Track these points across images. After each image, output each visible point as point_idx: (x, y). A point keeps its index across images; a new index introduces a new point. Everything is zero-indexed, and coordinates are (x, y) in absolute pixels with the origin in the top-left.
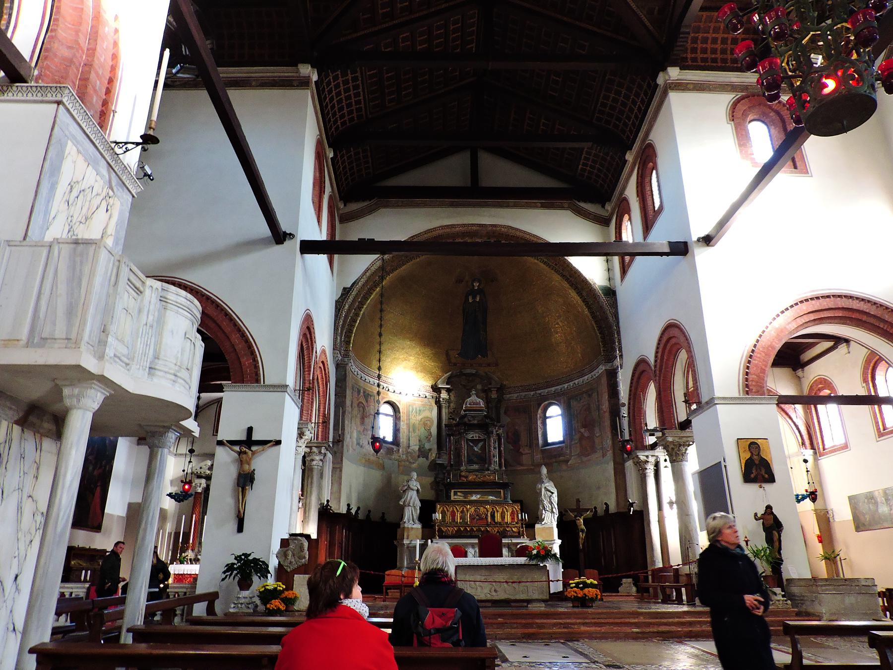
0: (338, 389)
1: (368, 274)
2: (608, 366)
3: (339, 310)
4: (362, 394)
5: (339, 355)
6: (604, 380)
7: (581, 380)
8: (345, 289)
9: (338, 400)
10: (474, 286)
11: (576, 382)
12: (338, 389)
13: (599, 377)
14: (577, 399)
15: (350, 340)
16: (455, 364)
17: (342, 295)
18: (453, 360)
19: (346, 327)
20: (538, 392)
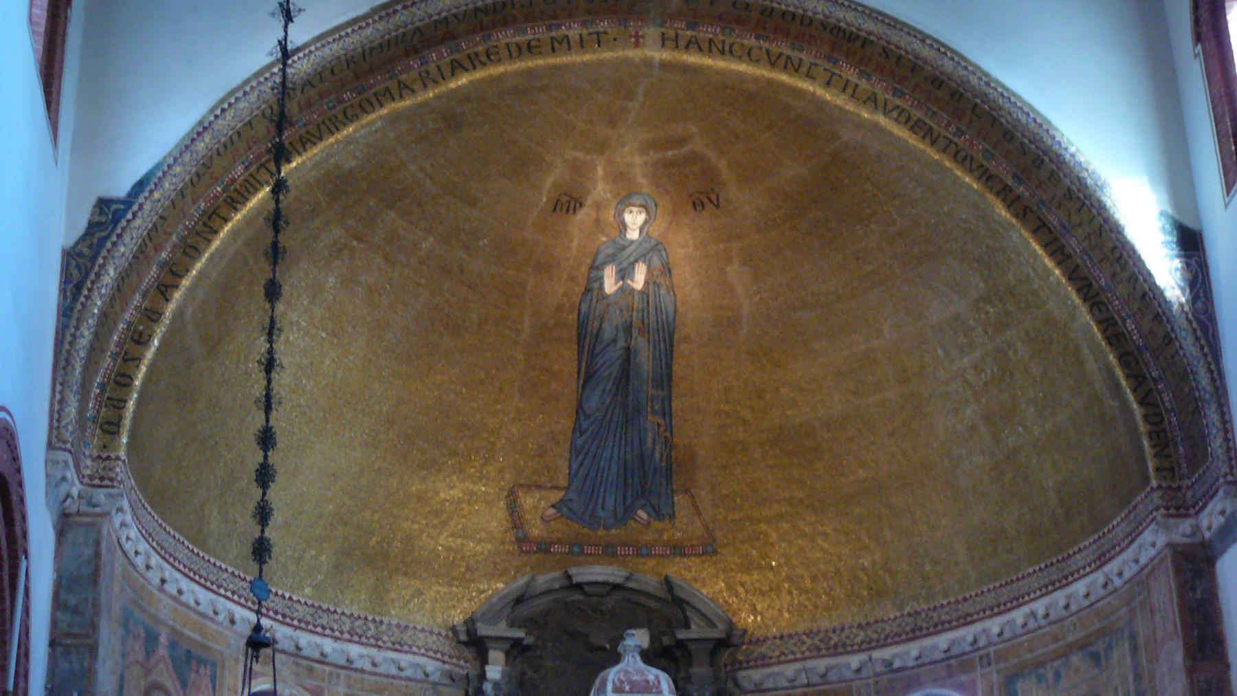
0: (65, 618)
1: (200, 146)
2: (1182, 530)
3: (78, 288)
4: (162, 651)
5: (71, 474)
6: (1164, 593)
7: (1060, 597)
8: (103, 204)
9: (64, 665)
10: (623, 227)
11: (1040, 606)
12: (65, 618)
13: (1142, 581)
14: (1041, 679)
15: (120, 418)
16: (544, 547)
17: (92, 227)
18: (536, 530)
19: (107, 361)
20: (876, 654)
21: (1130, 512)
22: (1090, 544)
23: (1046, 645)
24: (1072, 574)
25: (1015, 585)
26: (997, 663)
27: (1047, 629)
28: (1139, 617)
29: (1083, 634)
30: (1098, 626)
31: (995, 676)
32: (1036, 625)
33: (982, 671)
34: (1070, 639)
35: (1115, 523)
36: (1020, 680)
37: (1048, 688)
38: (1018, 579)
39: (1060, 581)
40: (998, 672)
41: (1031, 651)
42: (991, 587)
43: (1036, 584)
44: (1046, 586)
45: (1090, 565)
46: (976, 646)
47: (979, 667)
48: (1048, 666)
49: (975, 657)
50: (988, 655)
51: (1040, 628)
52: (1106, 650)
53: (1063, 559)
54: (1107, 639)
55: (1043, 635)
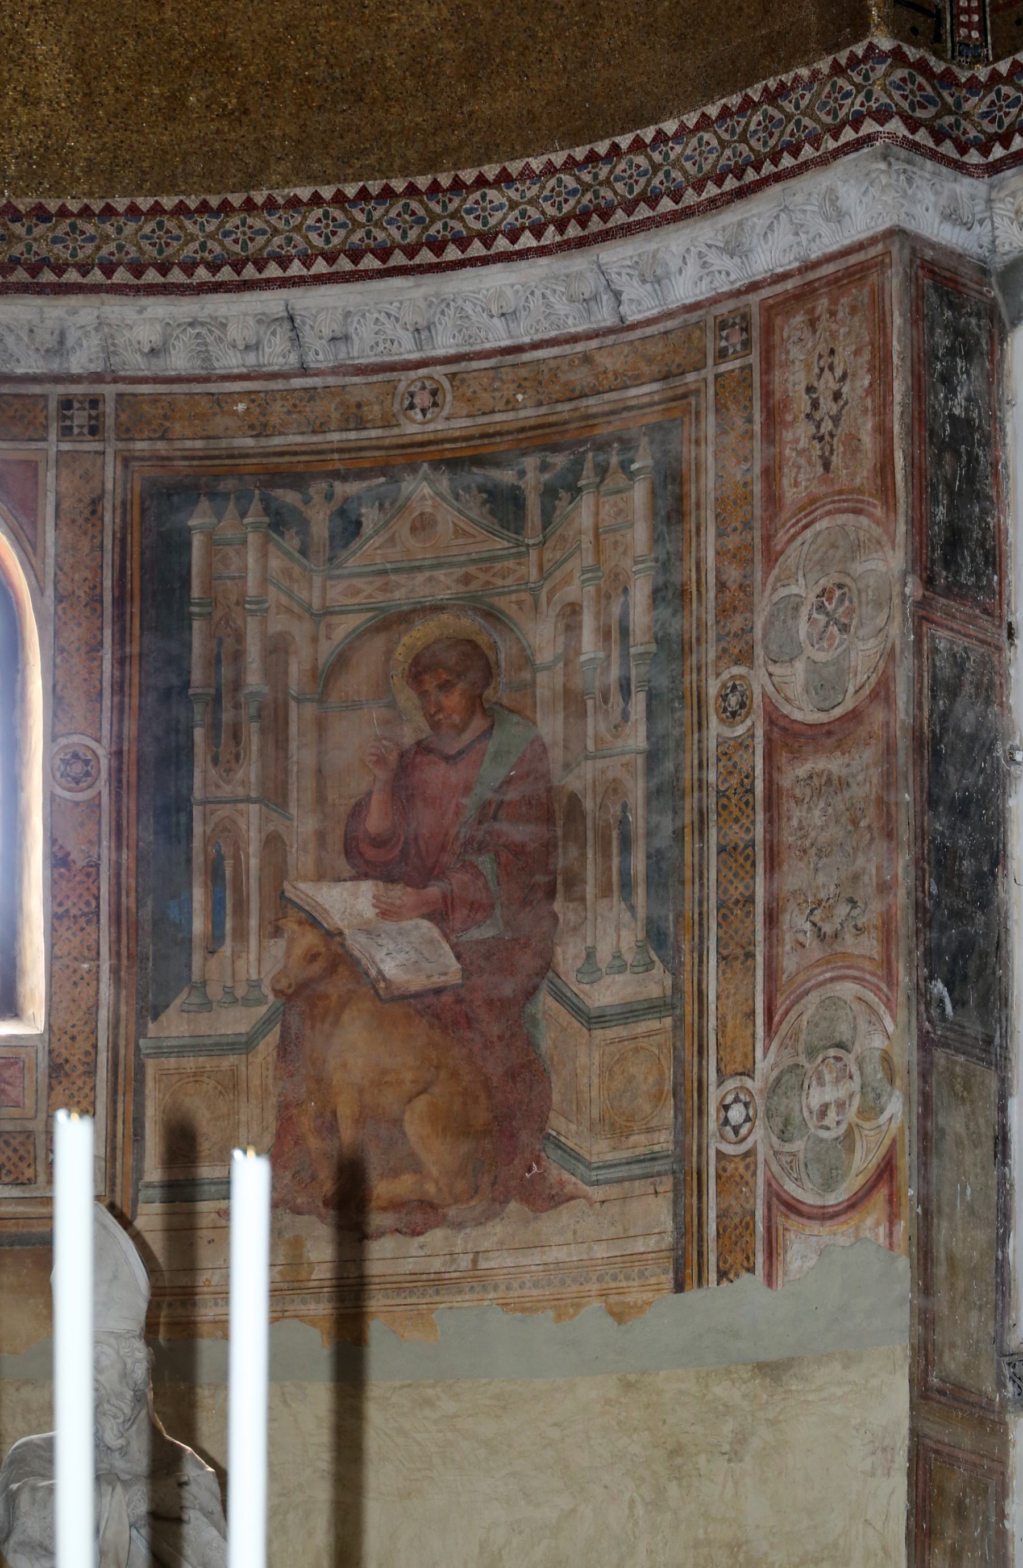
21: (748, 104)
22: (550, 170)
23: (321, 428)
24: (463, 243)
25: (235, 220)
26: (125, 433)
27: (331, 380)
28: (710, 423)
29: (461, 425)
30: (529, 414)
31: (111, 471)
32: (293, 359)
33: (65, 446)
34: (412, 428)
35: (670, 127)
36: (204, 504)
37: (303, 552)
38: (249, 206)
39: (411, 251)
40: (126, 460)
41: (261, 430)
42: (145, 203)
43: (318, 242)
44: (356, 256)
45: (538, 231)
46: (55, 366)
47: (53, 436)
48: (317, 489)
49: (44, 397)
50: (95, 402)
51: (304, 371)
52: (549, 493)
53: (435, 188)
54: (560, 460)
55: (311, 392)
